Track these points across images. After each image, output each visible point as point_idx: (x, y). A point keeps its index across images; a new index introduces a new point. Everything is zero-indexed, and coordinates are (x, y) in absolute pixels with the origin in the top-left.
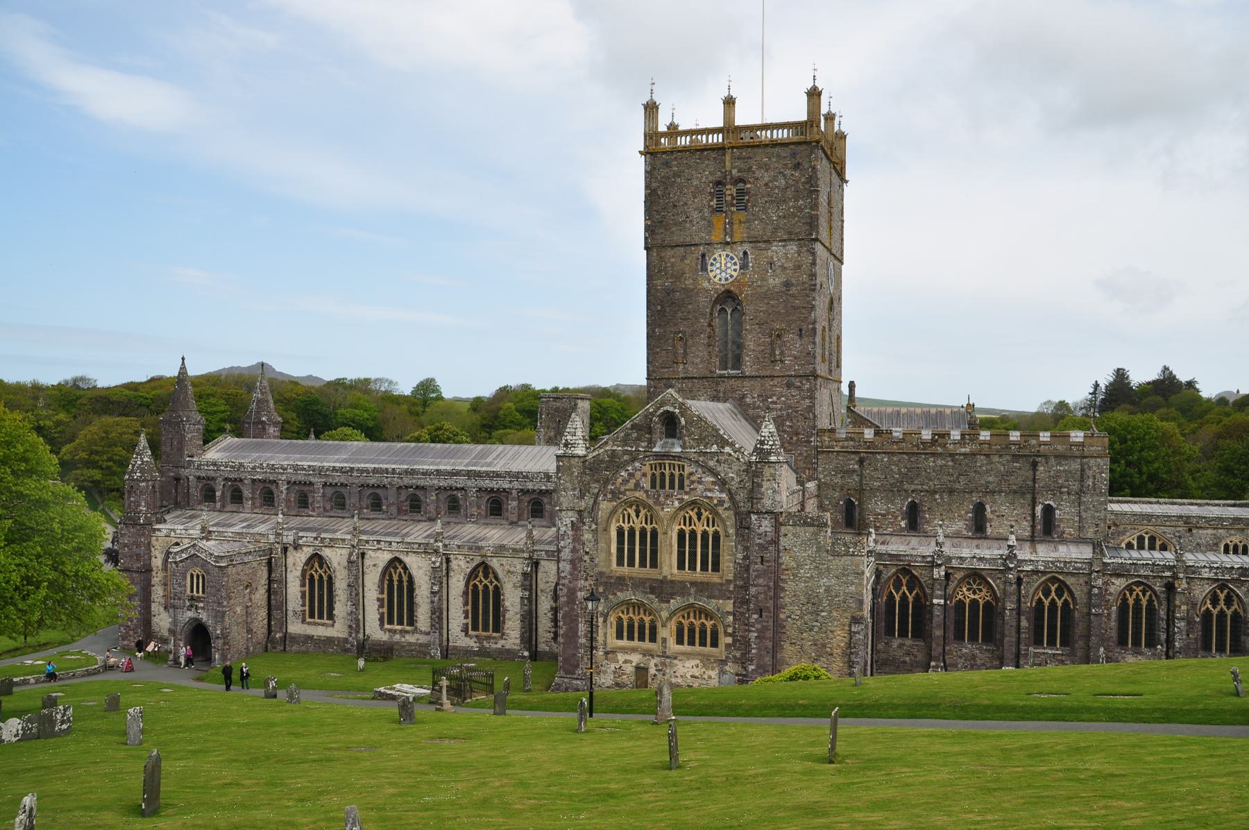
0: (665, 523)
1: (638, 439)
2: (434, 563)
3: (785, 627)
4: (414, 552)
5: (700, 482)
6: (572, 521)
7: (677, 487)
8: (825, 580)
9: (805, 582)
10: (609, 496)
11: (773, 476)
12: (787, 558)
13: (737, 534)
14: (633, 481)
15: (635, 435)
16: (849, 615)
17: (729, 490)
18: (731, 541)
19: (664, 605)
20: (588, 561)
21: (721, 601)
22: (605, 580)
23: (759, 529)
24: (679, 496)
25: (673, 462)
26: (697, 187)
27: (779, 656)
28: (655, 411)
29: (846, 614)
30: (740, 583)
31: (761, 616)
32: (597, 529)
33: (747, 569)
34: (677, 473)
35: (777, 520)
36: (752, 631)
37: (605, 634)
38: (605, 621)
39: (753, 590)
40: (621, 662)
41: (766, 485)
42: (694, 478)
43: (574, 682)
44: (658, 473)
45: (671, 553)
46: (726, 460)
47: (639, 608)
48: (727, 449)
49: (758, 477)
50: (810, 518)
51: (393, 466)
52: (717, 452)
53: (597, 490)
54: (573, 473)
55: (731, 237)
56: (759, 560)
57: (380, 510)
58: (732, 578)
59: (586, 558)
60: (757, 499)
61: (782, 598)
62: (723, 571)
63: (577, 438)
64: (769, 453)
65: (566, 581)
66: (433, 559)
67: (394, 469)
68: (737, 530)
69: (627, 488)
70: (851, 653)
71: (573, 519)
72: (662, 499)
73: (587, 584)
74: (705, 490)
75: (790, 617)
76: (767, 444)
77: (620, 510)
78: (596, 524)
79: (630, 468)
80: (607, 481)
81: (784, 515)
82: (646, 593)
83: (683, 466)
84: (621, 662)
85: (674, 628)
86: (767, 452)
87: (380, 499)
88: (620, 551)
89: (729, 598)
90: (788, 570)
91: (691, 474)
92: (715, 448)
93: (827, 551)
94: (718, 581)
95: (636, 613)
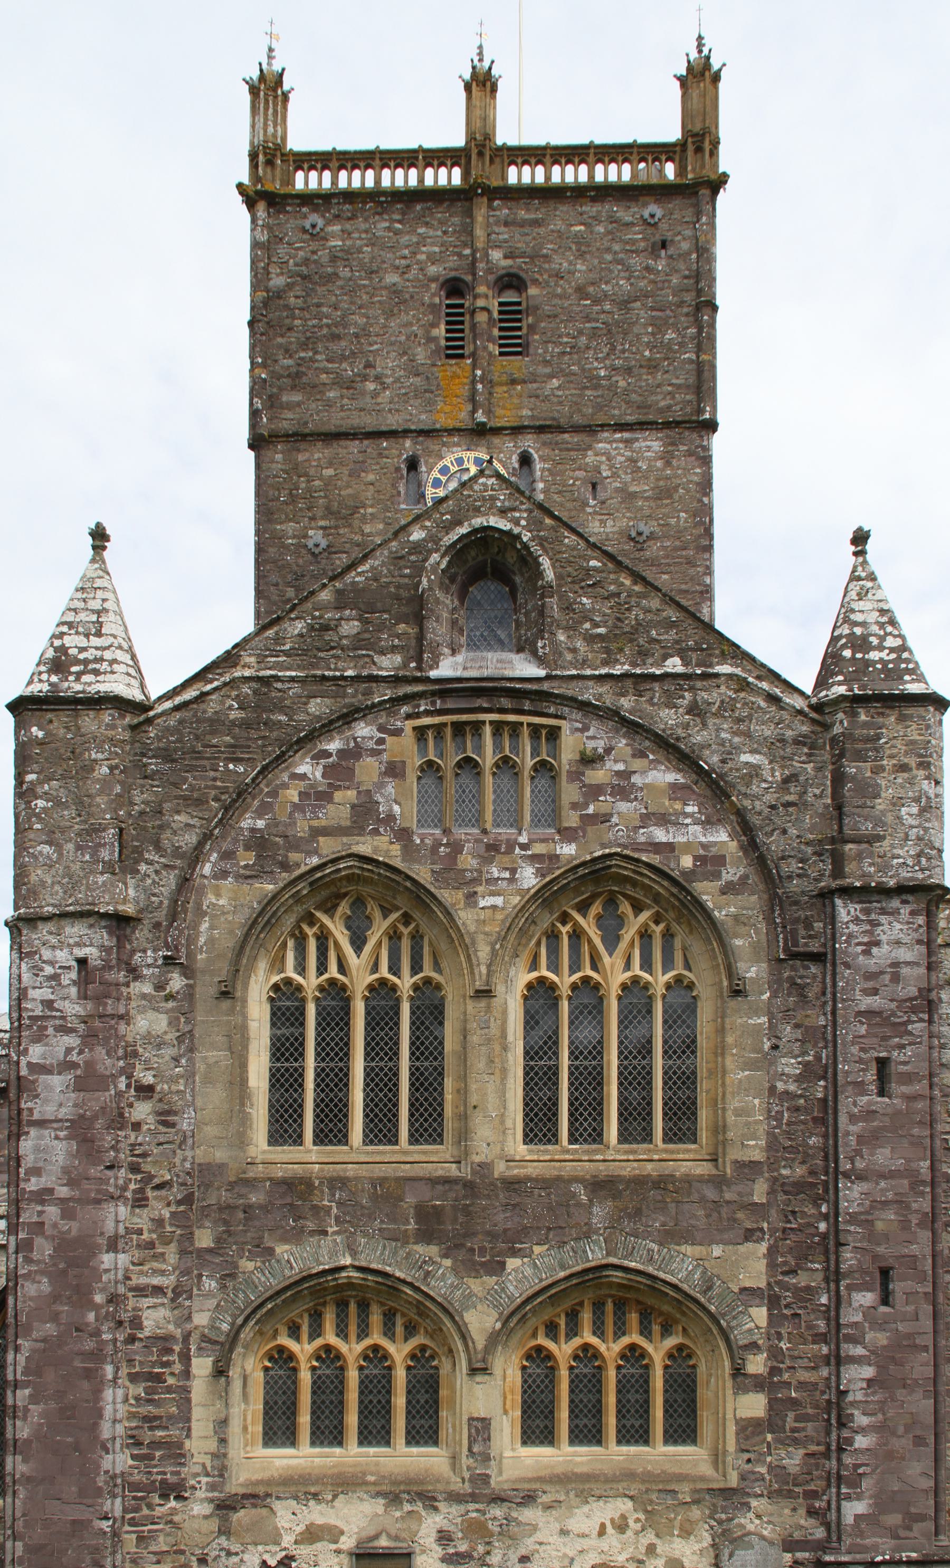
0: (483, 952)
6: (82, 962)
20: (151, 1122)
21: (717, 1251)
23: (867, 953)
26: (394, 291)
32: (189, 993)
40: (288, 1540)
46: (727, 706)
47: (364, 1306)
55: (489, 412)
62: (719, 1129)
73: (142, 1219)
74: (647, 819)
77: (289, 921)
78: (187, 971)
84: (288, 1540)
89: (750, 1235)
94: (703, 1169)
95: (353, 1329)
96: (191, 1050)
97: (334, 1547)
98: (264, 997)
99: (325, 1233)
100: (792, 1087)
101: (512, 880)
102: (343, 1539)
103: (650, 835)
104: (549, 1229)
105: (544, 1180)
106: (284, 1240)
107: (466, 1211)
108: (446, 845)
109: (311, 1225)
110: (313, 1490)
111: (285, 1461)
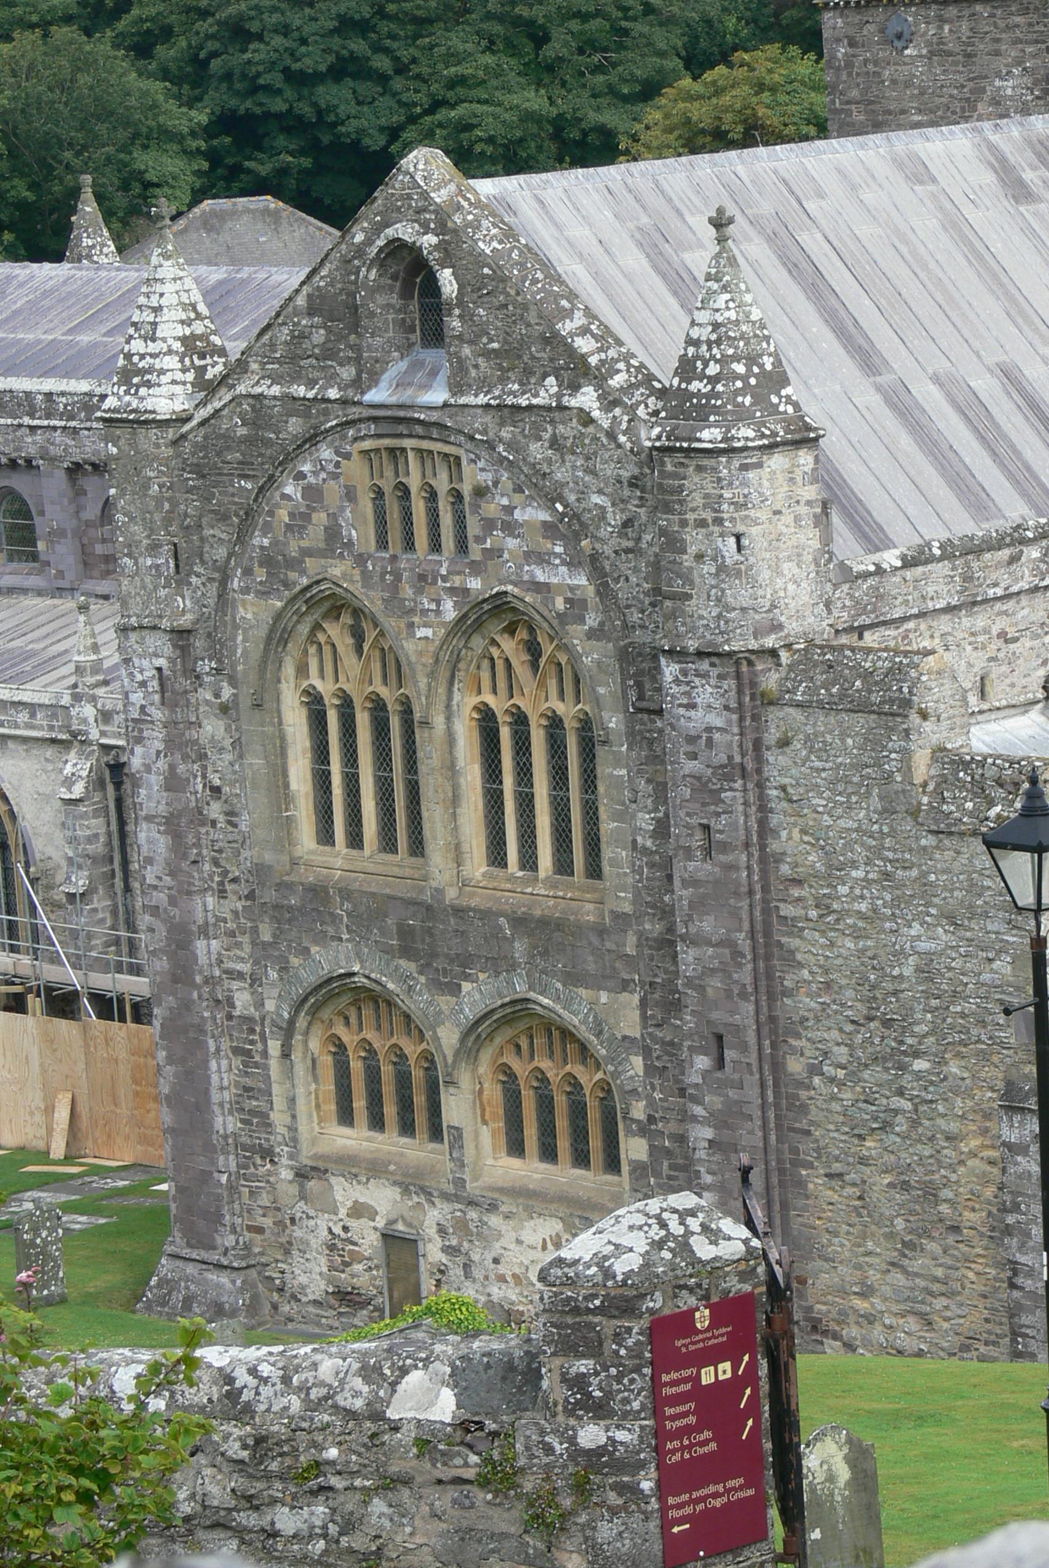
1: (328, 353)
2: (69, 782)
3: (804, 1109)
4: (25, 740)
5: (510, 528)
6: (159, 669)
7: (448, 541)
8: (916, 929)
9: (857, 934)
10: (261, 575)
11: (713, 503)
12: (796, 834)
13: (633, 736)
14: (320, 518)
15: (319, 336)
16: (995, 1075)
17: (595, 559)
18: (617, 764)
19: (445, 1002)
21: (604, 997)
22: (270, 895)
24: (457, 581)
25: (425, 445)
27: (795, 1224)
28: (369, 242)
29: (987, 1072)
30: (653, 928)
31: (720, 1063)
33: (665, 869)
34: (442, 483)
35: (746, 684)
36: (694, 1119)
37: (292, 1101)
38: (286, 1055)
39: (688, 957)
40: (343, 1212)
41: (694, 540)
42: (492, 508)
43: (212, 1276)
44: (387, 486)
45: (455, 800)
48: (587, 398)
49: (667, 508)
50: (867, 675)
51: (50, 385)
52: (549, 409)
53: (221, 553)
54: (146, 487)
56: (697, 840)
57: (34, 557)
58: (627, 908)
59: (215, 811)
60: (673, 597)
61: (787, 993)
63: (152, 347)
64: (702, 413)
65: (160, 898)
66: (68, 769)
67: (49, 395)
68: (630, 720)
69: (305, 544)
70: (1008, 1230)
71: (161, 662)
72: (408, 592)
75: (815, 1070)
76: (702, 377)
77: (304, 629)
78: (233, 681)
79: (306, 468)
80: (249, 515)
81: (785, 657)
82: (388, 951)
83: (458, 459)
84: (343, 1212)
85: (494, 1092)
86: (699, 405)
87: (28, 516)
88: (322, 781)
89: (625, 986)
90: (798, 882)
91: (480, 492)
92: (548, 391)
93: (914, 813)
96: (241, 757)
97: (372, 1224)
98: (297, 703)
99: (341, 939)
100: (649, 843)
101: (438, 612)
102: (378, 1218)
103: (531, 573)
104: (487, 959)
105: (480, 911)
106: (316, 942)
107: (429, 932)
108: (390, 573)
109: (331, 931)
110: (353, 1171)
111: (344, 1141)
